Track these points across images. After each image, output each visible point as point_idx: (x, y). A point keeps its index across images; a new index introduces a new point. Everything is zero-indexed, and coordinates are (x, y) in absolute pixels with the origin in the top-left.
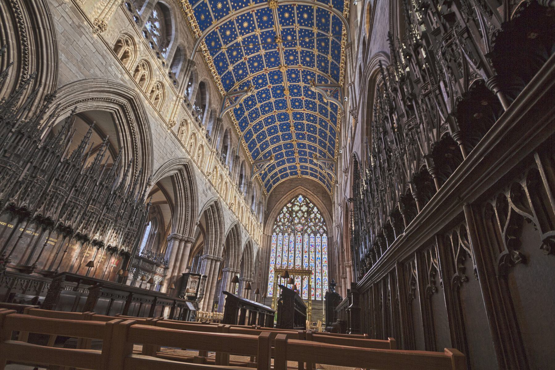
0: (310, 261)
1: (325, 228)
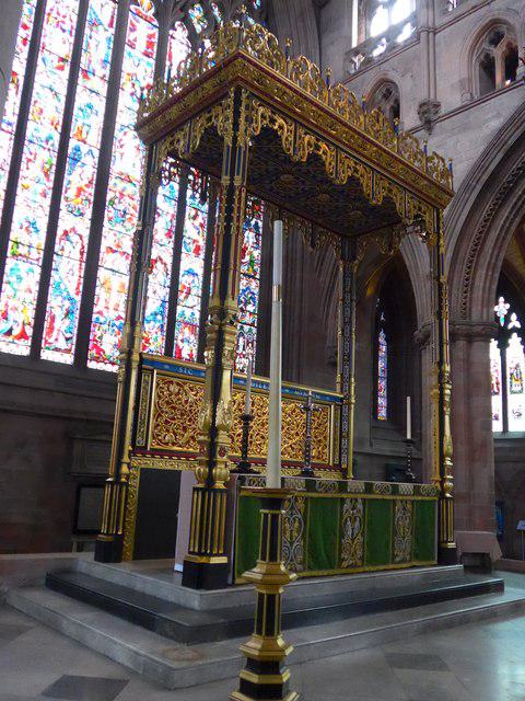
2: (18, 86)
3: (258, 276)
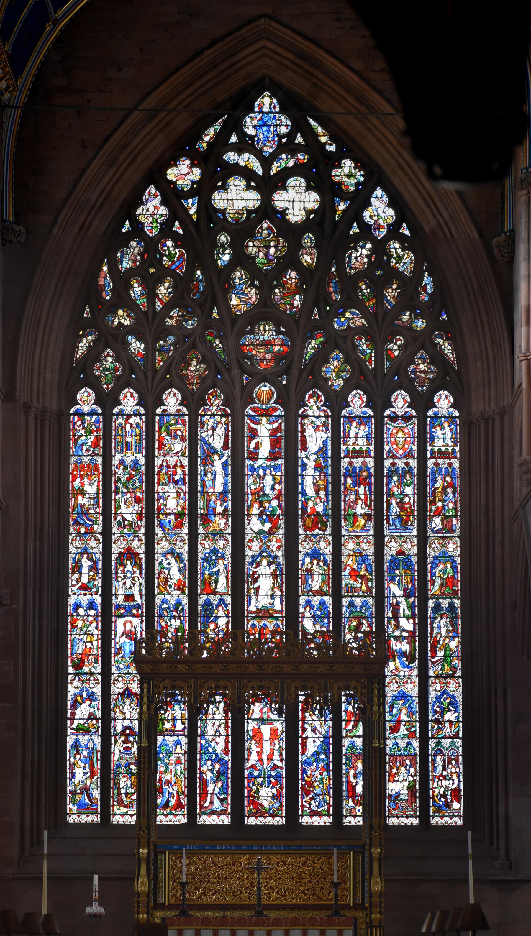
0: (347, 581)
1: (447, 349)
2: (141, 565)
3: (459, 673)
